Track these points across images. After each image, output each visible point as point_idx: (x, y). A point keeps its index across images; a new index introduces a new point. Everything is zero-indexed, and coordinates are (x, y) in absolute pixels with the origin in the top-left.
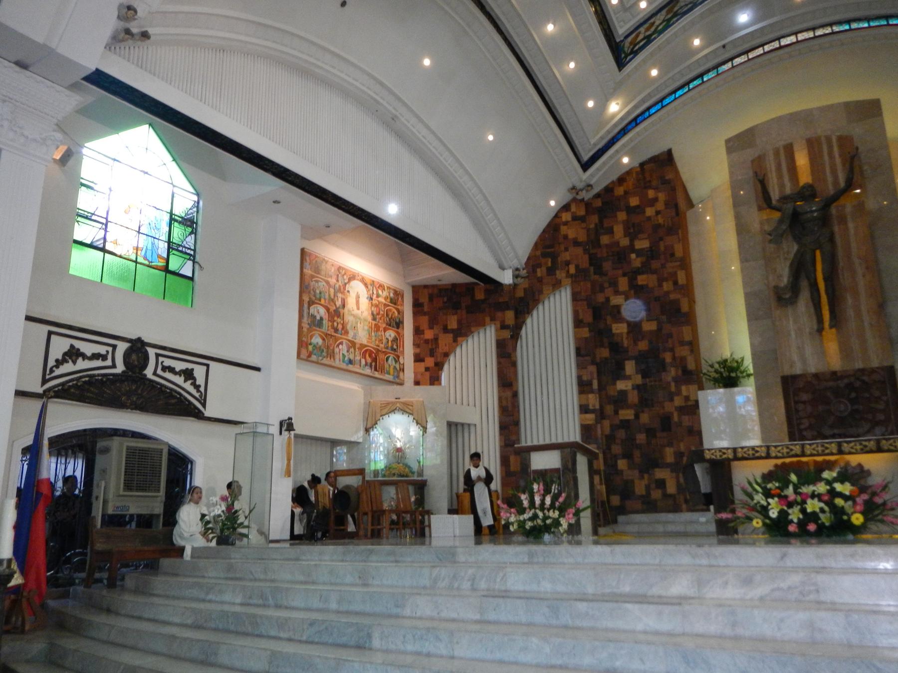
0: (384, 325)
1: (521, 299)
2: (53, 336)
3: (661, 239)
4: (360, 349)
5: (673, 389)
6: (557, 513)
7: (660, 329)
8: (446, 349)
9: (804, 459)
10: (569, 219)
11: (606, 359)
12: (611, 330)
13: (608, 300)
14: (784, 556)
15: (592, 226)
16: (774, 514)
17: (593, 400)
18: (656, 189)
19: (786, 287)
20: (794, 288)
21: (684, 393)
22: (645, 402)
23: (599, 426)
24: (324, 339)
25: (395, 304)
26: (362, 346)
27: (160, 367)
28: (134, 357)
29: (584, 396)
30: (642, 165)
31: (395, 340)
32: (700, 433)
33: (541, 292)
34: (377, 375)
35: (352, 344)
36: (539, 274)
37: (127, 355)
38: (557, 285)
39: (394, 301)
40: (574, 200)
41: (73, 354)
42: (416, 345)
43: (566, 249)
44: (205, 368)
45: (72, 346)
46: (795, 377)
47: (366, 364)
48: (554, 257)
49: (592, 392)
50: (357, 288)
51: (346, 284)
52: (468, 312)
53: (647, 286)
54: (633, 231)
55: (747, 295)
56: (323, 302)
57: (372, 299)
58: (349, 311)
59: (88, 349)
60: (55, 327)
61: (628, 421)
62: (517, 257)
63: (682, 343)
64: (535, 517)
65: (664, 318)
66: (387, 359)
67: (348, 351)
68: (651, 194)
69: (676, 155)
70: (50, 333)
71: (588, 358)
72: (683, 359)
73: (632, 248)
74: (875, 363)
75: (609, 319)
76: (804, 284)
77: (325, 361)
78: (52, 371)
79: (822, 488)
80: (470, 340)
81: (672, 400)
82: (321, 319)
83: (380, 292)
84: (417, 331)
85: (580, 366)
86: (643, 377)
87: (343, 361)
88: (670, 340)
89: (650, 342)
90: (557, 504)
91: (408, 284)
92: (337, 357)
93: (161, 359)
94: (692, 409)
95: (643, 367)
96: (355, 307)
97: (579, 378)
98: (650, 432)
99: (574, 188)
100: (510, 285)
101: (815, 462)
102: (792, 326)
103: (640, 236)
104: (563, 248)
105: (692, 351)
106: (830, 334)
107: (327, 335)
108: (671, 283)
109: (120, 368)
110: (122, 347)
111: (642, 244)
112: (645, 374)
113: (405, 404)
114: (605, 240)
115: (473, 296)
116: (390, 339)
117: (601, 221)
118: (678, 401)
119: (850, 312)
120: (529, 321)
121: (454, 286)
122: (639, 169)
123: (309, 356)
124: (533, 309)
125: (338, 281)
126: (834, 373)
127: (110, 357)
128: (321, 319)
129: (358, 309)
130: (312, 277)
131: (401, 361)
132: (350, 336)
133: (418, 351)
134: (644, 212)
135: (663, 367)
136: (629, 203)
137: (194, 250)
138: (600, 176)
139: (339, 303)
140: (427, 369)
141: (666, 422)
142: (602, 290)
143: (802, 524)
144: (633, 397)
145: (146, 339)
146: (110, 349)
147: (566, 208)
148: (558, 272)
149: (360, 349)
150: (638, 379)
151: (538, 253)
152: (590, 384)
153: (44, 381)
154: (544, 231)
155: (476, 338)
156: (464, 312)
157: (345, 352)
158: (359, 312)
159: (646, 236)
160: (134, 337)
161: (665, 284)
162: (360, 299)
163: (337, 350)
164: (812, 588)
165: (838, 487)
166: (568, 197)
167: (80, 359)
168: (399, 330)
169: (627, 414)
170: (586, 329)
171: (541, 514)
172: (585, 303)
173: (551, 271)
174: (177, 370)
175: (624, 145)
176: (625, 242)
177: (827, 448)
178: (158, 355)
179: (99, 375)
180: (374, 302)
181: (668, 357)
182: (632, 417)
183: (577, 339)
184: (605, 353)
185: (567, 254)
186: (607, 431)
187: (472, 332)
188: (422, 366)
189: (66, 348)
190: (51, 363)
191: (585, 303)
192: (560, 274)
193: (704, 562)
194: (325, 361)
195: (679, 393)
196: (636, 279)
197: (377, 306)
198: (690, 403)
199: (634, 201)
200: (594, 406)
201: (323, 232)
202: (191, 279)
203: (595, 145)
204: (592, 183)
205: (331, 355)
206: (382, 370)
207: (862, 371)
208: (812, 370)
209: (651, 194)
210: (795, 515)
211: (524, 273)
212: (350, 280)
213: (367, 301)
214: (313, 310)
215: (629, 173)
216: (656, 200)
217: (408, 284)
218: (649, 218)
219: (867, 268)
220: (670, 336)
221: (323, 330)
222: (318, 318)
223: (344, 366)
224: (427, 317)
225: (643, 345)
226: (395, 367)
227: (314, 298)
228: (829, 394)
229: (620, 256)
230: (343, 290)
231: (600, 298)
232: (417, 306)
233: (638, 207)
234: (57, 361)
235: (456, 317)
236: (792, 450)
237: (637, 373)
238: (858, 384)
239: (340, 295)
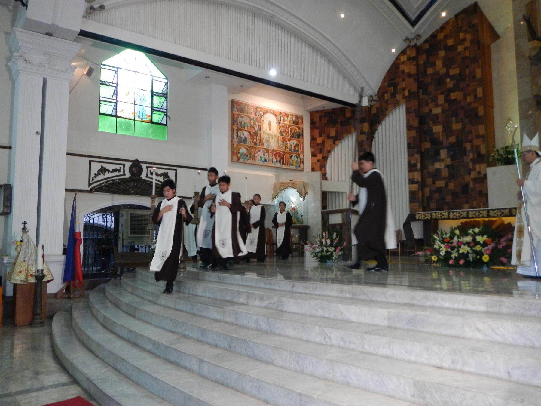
0: (289, 138)
1: (375, 114)
2: (92, 163)
3: (467, 67)
4: (272, 153)
5: (471, 167)
6: (333, 249)
7: (464, 128)
8: (329, 148)
9: (478, 219)
10: (405, 59)
11: (428, 149)
12: (432, 130)
13: (431, 111)
14: (293, 286)
15: (422, 62)
16: (442, 253)
17: (417, 176)
18: (465, 32)
21: (478, 169)
22: (452, 176)
23: (420, 192)
24: (248, 150)
25: (297, 124)
27: (149, 173)
28: (134, 169)
29: (411, 173)
30: (456, 16)
31: (297, 145)
32: (486, 195)
33: (387, 109)
34: (284, 166)
35: (267, 150)
36: (386, 98)
37: (131, 169)
38: (397, 104)
39: (295, 123)
40: (409, 47)
41: (103, 170)
42: (312, 146)
43: (403, 80)
44: (175, 171)
45: (102, 167)
47: (277, 161)
48: (395, 86)
49: (416, 170)
50: (270, 118)
51: (261, 117)
52: (341, 126)
53: (456, 99)
54: (448, 63)
55: (520, 102)
56: (246, 128)
57: (280, 123)
58: (264, 132)
59: (110, 167)
60: (93, 158)
61: (441, 188)
62: (371, 88)
63: (478, 137)
64: (322, 251)
65: (467, 120)
66: (291, 157)
68: (462, 36)
69: (481, 5)
70: (90, 161)
71: (415, 150)
72: (478, 147)
73: (447, 75)
75: (431, 123)
77: (248, 162)
78: (93, 179)
79: (469, 239)
80: (343, 142)
81: (470, 174)
82: (246, 138)
83: (286, 118)
84: (313, 139)
85: (410, 155)
86: (451, 160)
87: (261, 161)
88: (470, 135)
89: (457, 137)
90: (334, 244)
91: (307, 111)
92: (257, 158)
93: (149, 169)
94: (482, 179)
95: (452, 153)
96: (268, 129)
97: (409, 162)
98: (455, 194)
99: (407, 39)
100: (366, 107)
101: (484, 221)
103: (453, 66)
104: (401, 79)
105: (484, 141)
107: (249, 147)
108: (472, 96)
109: (128, 175)
110: (128, 165)
111: (454, 71)
112: (453, 158)
113: (293, 184)
114: (430, 71)
115: (344, 116)
116: (293, 145)
117: (428, 58)
118: (473, 175)
120: (380, 128)
121: (334, 110)
122: (454, 20)
123: (239, 159)
124: (382, 121)
125: (256, 115)
127: (122, 170)
128: (246, 138)
129: (270, 130)
130: (239, 115)
131: (301, 157)
132: (265, 146)
133: (313, 150)
134: (456, 49)
135: (464, 152)
136: (446, 44)
137: (167, 109)
138: (426, 28)
139: (257, 128)
140: (318, 161)
141: (465, 188)
142: (427, 104)
143: (457, 259)
144: (445, 173)
145: (140, 160)
146: (122, 166)
147: (403, 52)
148: (397, 95)
149: (272, 153)
150: (449, 161)
151: (386, 84)
152: (415, 165)
153: (90, 184)
154: (390, 69)
155: (346, 141)
156: (339, 125)
158: (271, 132)
159: (457, 65)
160: (134, 159)
161: (468, 97)
162: (272, 124)
163: (256, 155)
164: (281, 304)
165: (479, 239)
166: (405, 45)
167: (107, 172)
168: (300, 139)
169: (441, 184)
170: (414, 131)
171: (325, 249)
172: (414, 114)
173: (393, 95)
174: (159, 173)
175: (439, 5)
176: (443, 71)
177: (481, 214)
178: (147, 167)
179: (116, 180)
180: (281, 125)
181: (468, 146)
182: (444, 185)
183: (409, 138)
184: (427, 145)
185: (404, 83)
186: (427, 194)
187: (343, 138)
188: (316, 159)
189: (99, 168)
190: (92, 175)
191: (414, 114)
192: (399, 97)
193: (268, 287)
194: (248, 162)
195: (474, 169)
196: (449, 95)
197: (283, 127)
198: (481, 176)
199: (450, 42)
200: (418, 179)
201: (242, 89)
202: (166, 125)
203: (418, 8)
204: (420, 34)
205: (253, 158)
206: (288, 164)
209: (462, 36)
210: (454, 255)
211: (375, 98)
212: (264, 114)
214: (239, 134)
215: (447, 23)
216: (465, 39)
217: (307, 111)
218: (460, 53)
220: (470, 132)
222: (243, 138)
223: (261, 163)
224: (318, 130)
225: (452, 139)
226: (297, 161)
227: (240, 127)
229: (440, 81)
230: (260, 120)
231: (426, 110)
232: (313, 124)
233: (452, 46)
234: (95, 174)
235: (334, 129)
236: (461, 214)
237: (448, 157)
239: (257, 124)
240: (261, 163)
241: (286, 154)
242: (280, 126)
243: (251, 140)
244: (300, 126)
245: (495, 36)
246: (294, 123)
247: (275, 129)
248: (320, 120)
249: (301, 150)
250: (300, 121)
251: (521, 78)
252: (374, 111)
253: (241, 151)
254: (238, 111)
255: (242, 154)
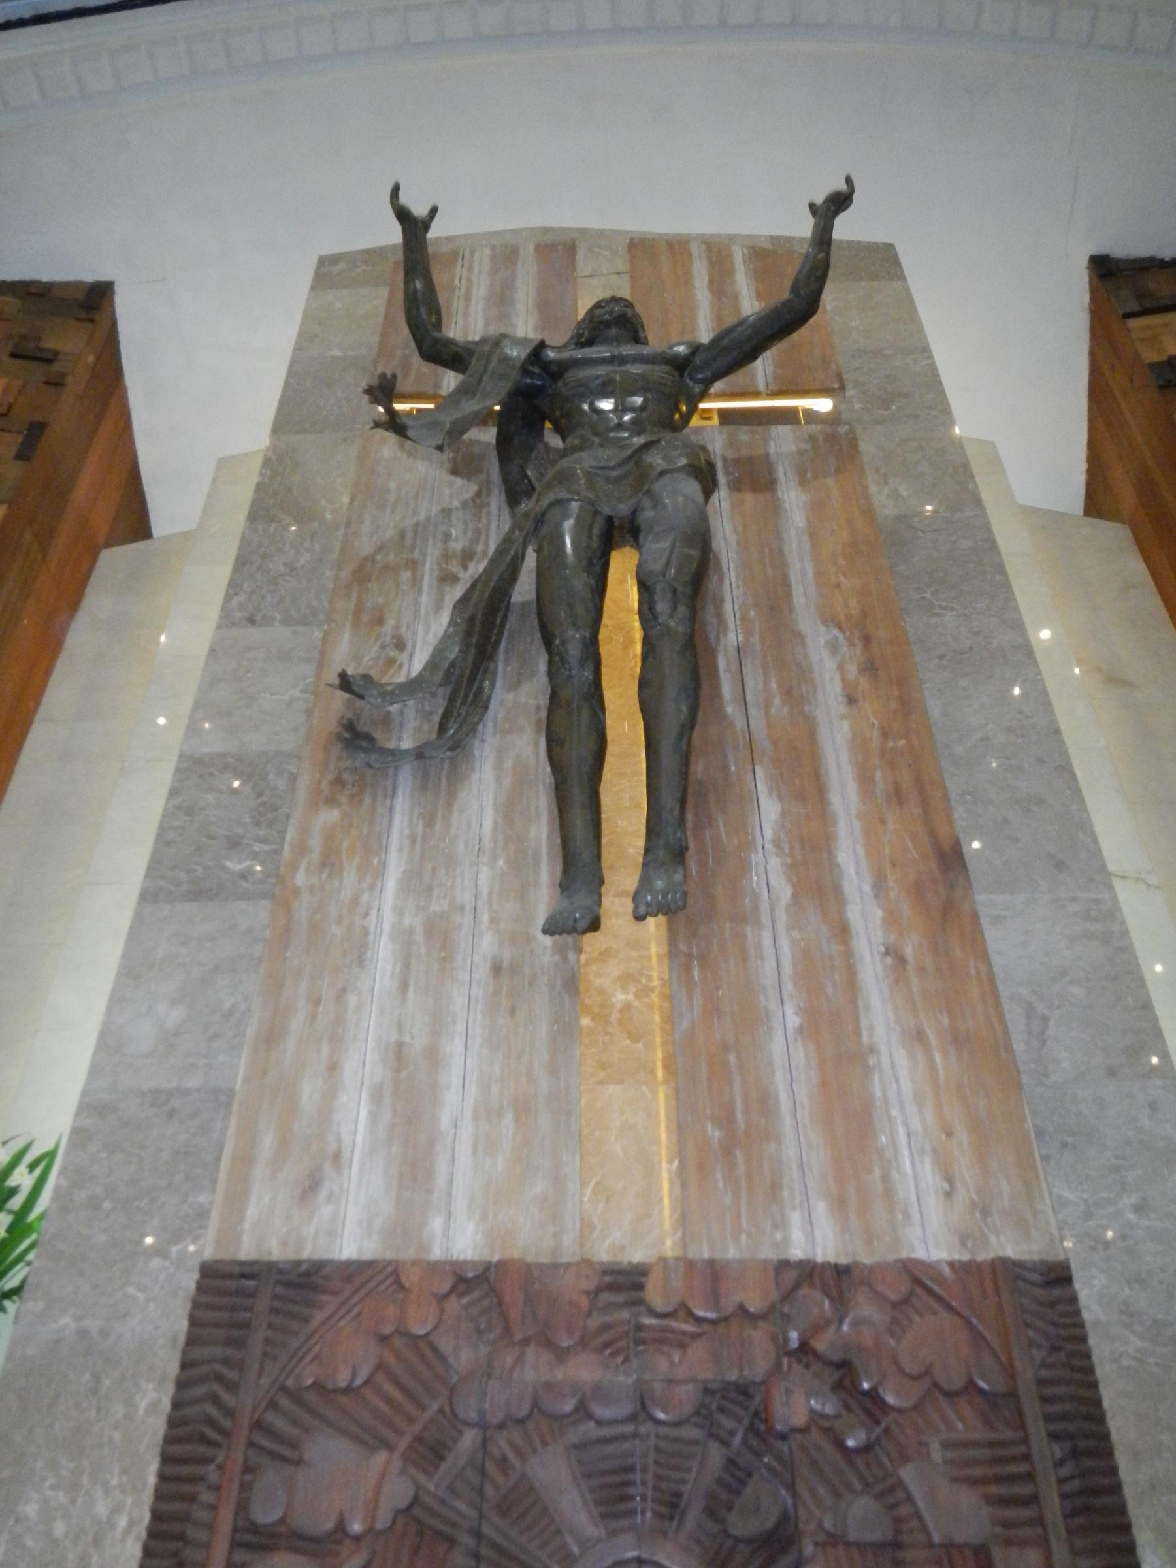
19: (414, 686)
20: (462, 687)
46: (302, 1285)
74: (930, 1234)
76: (518, 696)
102: (388, 909)
106: (631, 949)
119: (770, 875)
126: (626, 1282)
207: (837, 1280)
208: (460, 1238)
219: (870, 668)
228: (555, 1475)
238: (800, 1403)
245: (134, 522)
251: (251, 621)
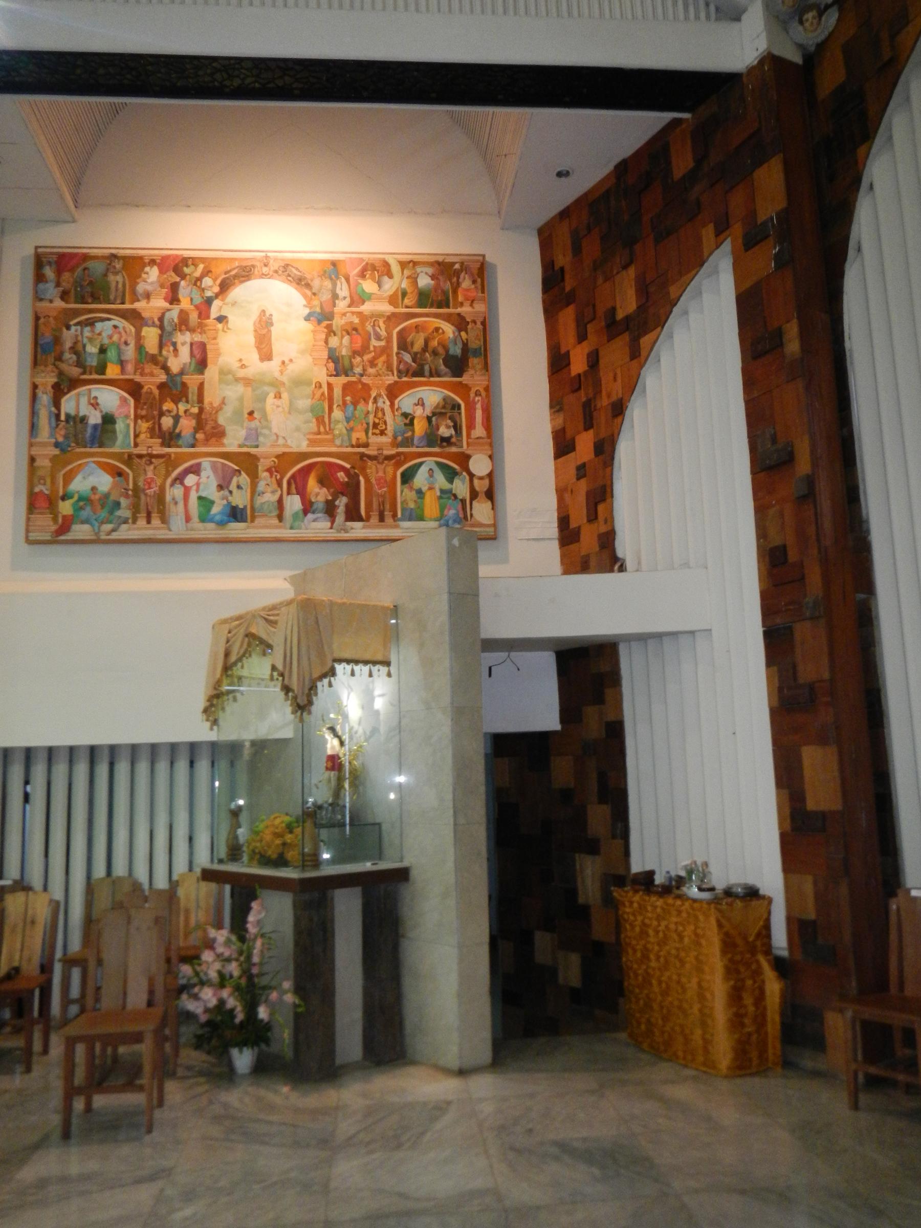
0: (391, 379)
25: (444, 304)
26: (285, 459)
31: (447, 410)
34: (358, 529)
35: (247, 462)
47: (308, 507)
51: (209, 302)
56: (112, 372)
58: (224, 372)
66: (407, 478)
67: (220, 487)
77: (125, 532)
82: (109, 420)
83: (369, 286)
107: (129, 459)
123: (64, 528)
125: (174, 299)
128: (109, 420)
129: (266, 356)
131: (480, 465)
139: (179, 360)
157: (210, 490)
158: (273, 367)
168: (465, 379)
197: (350, 330)
205: (153, 508)
212: (225, 287)
213: (308, 326)
214: (68, 405)
221: (116, 449)
222: (95, 418)
226: (447, 494)
227: (75, 371)
239: (184, 339)
240: (209, 530)
241: (372, 469)
242: (330, 331)
243: (144, 426)
244: (465, 310)
246: (424, 298)
247: (297, 343)
248: (577, 249)
249: (479, 431)
250: (466, 283)
252: (831, 77)
253: (80, 485)
254: (64, 296)
255: (85, 500)
